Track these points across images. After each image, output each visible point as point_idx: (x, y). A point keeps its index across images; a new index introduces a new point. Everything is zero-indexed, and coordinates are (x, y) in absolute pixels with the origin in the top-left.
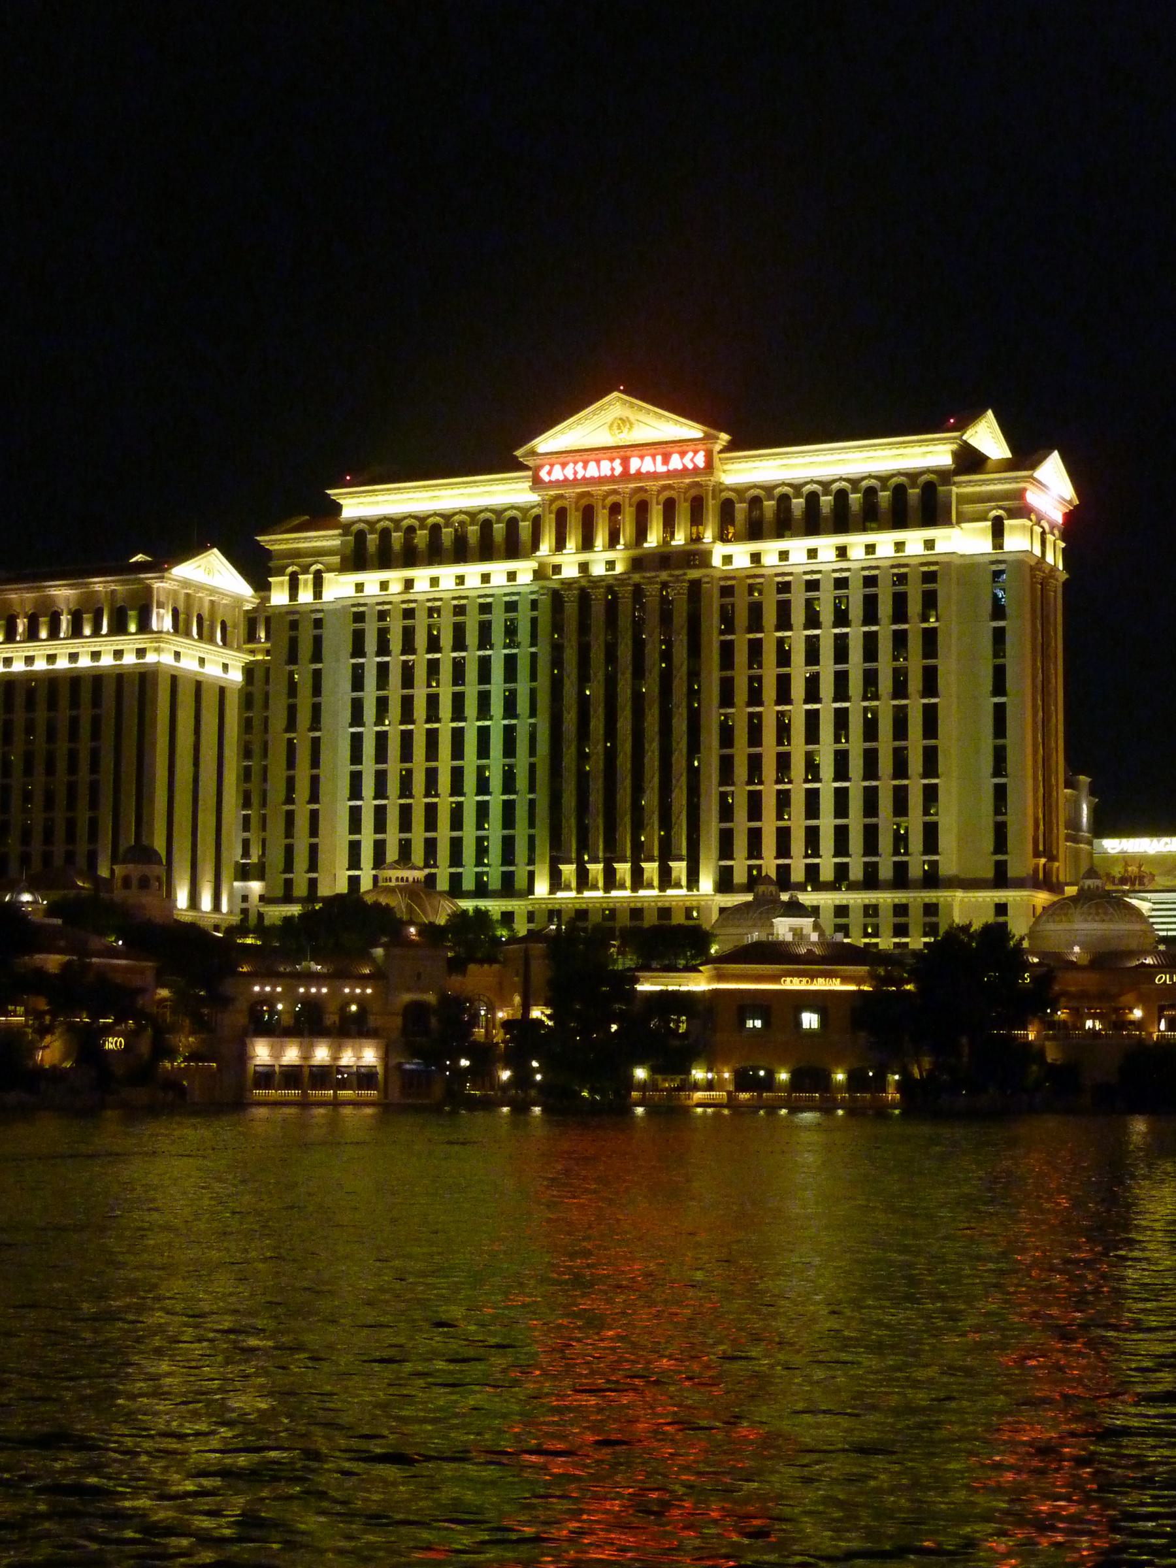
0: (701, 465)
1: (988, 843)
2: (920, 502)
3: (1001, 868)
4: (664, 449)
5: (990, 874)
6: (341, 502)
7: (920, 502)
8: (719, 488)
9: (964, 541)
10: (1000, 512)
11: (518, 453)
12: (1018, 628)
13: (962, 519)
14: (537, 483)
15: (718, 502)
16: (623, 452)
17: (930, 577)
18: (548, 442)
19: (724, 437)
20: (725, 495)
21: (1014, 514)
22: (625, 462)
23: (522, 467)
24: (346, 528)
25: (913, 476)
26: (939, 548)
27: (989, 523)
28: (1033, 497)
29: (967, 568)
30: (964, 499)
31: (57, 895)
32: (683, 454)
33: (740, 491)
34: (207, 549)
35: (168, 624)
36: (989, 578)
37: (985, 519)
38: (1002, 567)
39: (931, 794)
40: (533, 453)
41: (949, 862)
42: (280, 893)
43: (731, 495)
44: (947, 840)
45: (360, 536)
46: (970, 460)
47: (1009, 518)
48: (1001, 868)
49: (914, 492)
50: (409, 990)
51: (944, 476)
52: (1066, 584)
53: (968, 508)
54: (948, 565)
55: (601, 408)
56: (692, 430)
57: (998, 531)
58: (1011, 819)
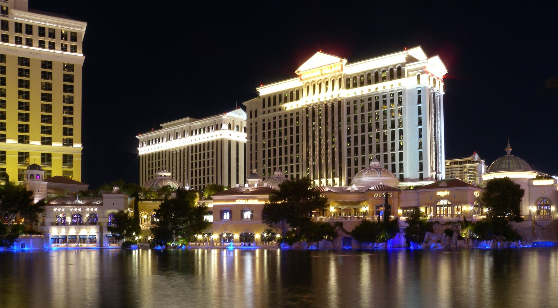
2: (397, 73)
7: (397, 73)
11: (296, 72)
12: (426, 105)
13: (408, 76)
14: (301, 79)
17: (400, 93)
19: (345, 61)
21: (422, 73)
23: (298, 76)
26: (402, 85)
28: (427, 69)
30: (409, 71)
34: (238, 108)
35: (227, 127)
37: (414, 75)
38: (420, 89)
40: (299, 72)
44: (406, 168)
46: (411, 60)
49: (395, 70)
50: (109, 208)
51: (403, 65)
52: (444, 95)
53: (410, 73)
54: (405, 90)
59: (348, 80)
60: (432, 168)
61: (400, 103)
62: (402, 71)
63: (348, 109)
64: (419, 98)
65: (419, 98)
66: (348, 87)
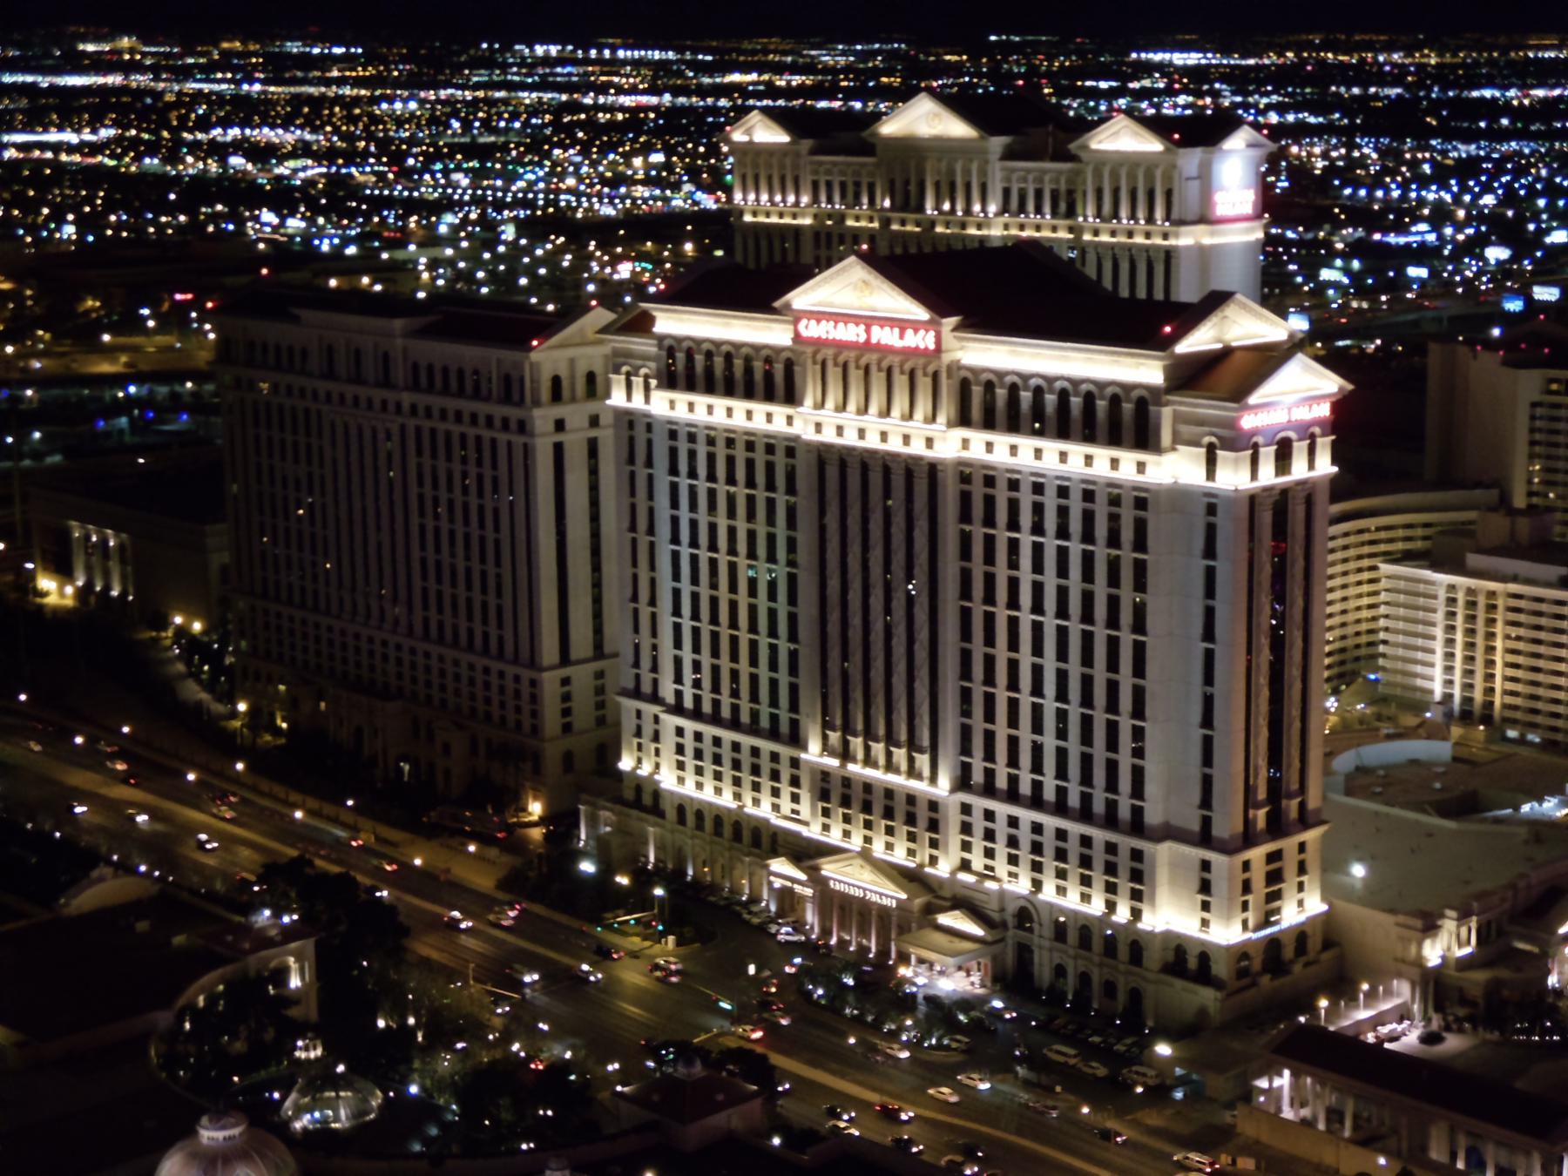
0: (932, 346)
1: (1196, 796)
3: (1206, 822)
4: (902, 325)
5: (1195, 826)
6: (655, 313)
8: (955, 367)
9: (1175, 468)
10: (1213, 439)
15: (956, 382)
16: (868, 322)
18: (801, 298)
20: (964, 373)
22: (868, 331)
24: (661, 339)
25: (1128, 388)
27: (1203, 450)
29: (1178, 496)
31: (285, 810)
32: (916, 331)
33: (976, 371)
36: (1202, 510)
39: (1138, 734)
41: (1154, 815)
42: (631, 685)
43: (969, 375)
44: (1150, 788)
45: (671, 352)
47: (1224, 448)
48: (1206, 822)
55: (843, 270)
56: (921, 313)
57: (1211, 462)
58: (1216, 772)
59: (964, 388)
60: (1249, 790)
61: (1140, 544)
62: (1152, 421)
63: (965, 498)
64: (1211, 531)
65: (1211, 531)
66: (964, 420)
